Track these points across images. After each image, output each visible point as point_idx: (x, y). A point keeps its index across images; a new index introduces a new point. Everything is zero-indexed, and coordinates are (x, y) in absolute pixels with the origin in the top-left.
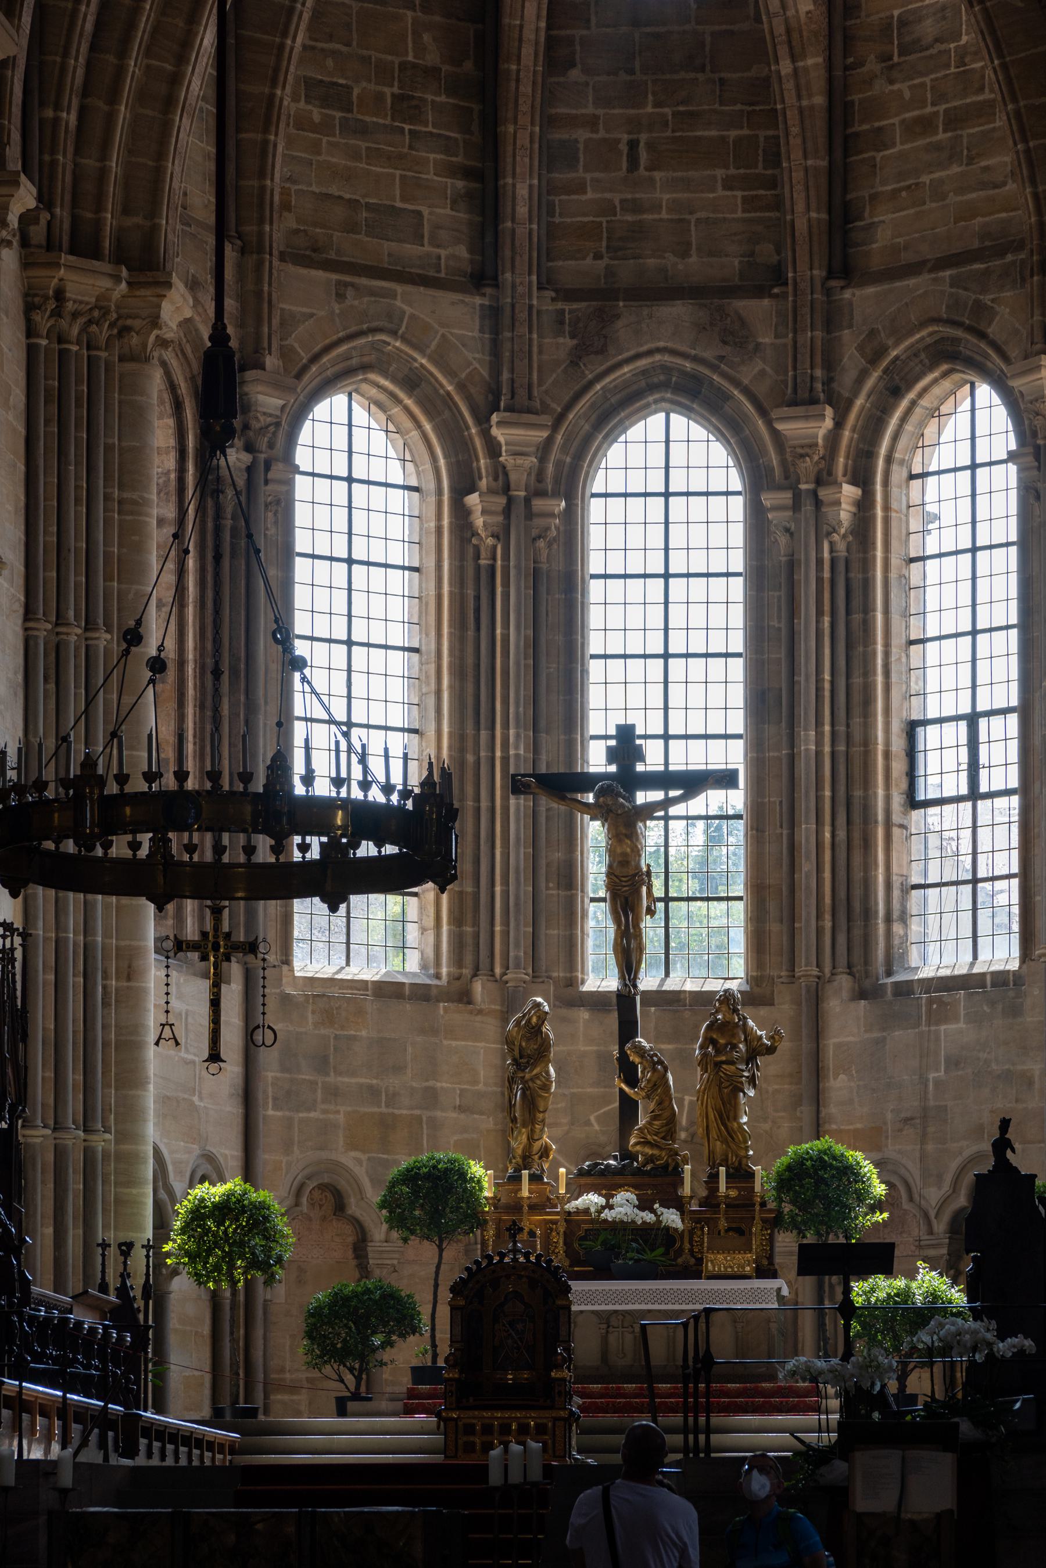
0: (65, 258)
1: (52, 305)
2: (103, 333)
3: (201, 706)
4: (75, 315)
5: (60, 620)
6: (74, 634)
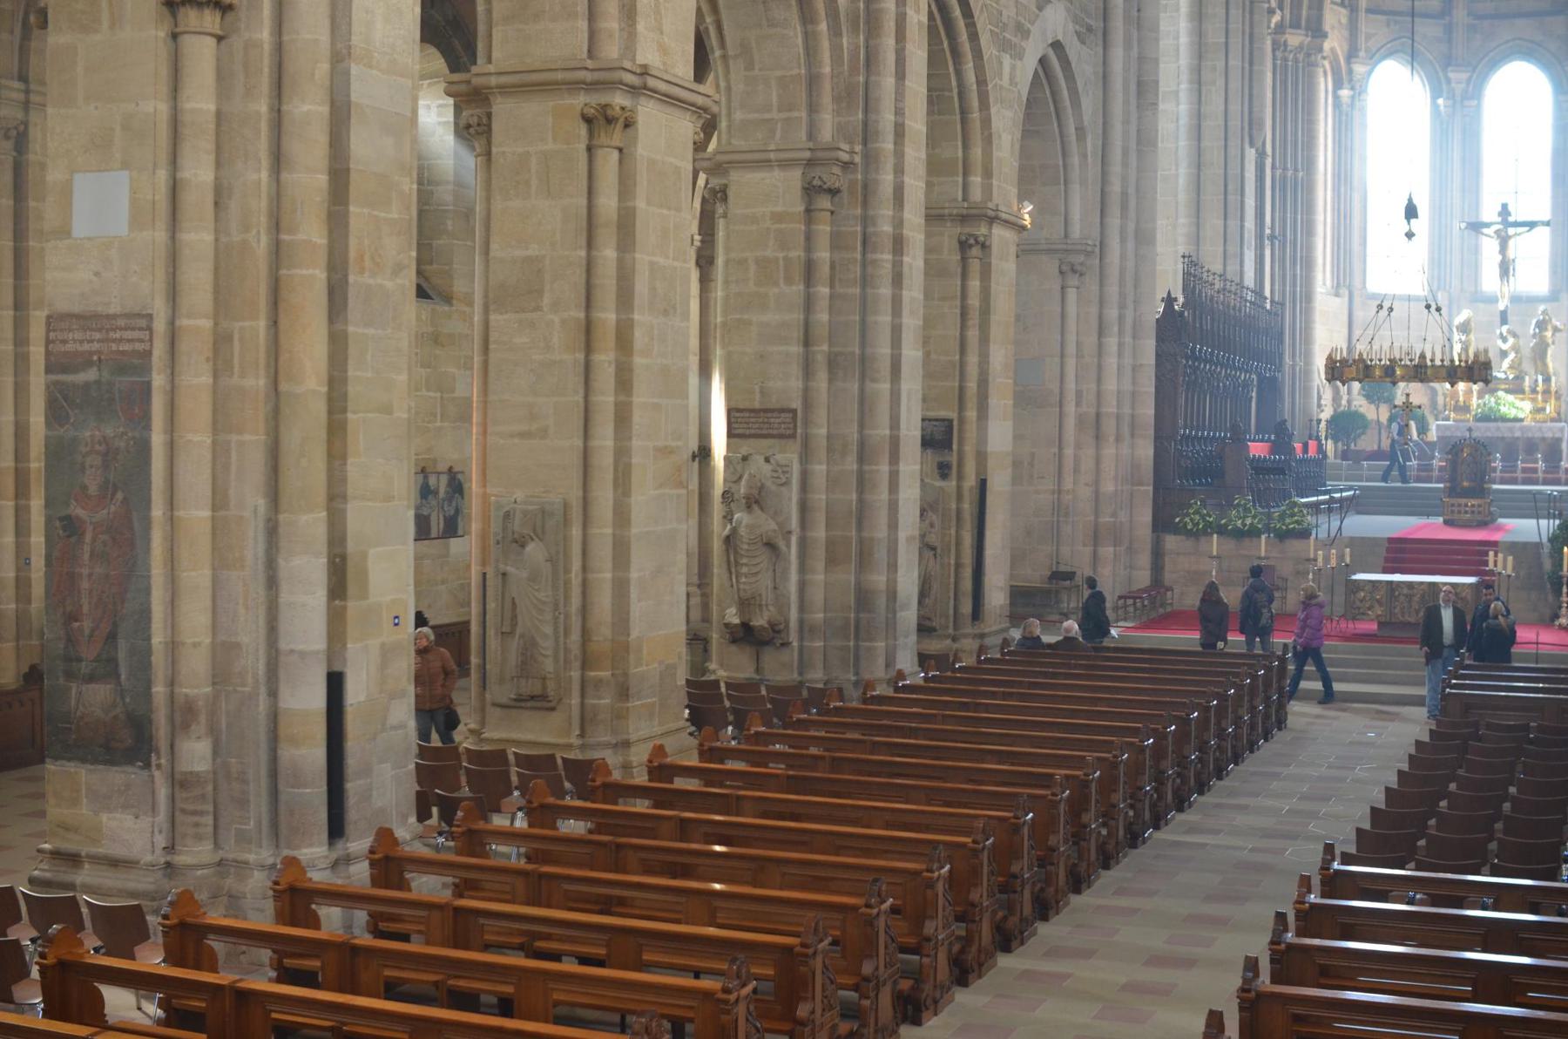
0: (1288, 30)
1: (1282, 48)
2: (1301, 57)
3: (1333, 190)
4: (1291, 51)
5: (1285, 169)
6: (1290, 173)
